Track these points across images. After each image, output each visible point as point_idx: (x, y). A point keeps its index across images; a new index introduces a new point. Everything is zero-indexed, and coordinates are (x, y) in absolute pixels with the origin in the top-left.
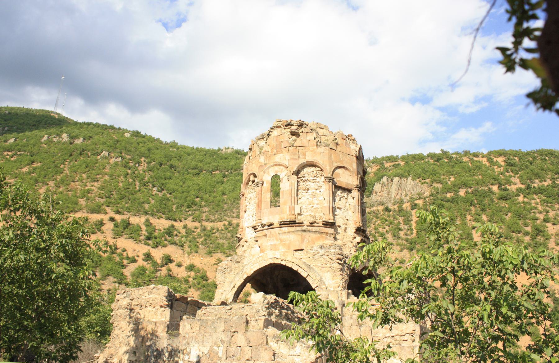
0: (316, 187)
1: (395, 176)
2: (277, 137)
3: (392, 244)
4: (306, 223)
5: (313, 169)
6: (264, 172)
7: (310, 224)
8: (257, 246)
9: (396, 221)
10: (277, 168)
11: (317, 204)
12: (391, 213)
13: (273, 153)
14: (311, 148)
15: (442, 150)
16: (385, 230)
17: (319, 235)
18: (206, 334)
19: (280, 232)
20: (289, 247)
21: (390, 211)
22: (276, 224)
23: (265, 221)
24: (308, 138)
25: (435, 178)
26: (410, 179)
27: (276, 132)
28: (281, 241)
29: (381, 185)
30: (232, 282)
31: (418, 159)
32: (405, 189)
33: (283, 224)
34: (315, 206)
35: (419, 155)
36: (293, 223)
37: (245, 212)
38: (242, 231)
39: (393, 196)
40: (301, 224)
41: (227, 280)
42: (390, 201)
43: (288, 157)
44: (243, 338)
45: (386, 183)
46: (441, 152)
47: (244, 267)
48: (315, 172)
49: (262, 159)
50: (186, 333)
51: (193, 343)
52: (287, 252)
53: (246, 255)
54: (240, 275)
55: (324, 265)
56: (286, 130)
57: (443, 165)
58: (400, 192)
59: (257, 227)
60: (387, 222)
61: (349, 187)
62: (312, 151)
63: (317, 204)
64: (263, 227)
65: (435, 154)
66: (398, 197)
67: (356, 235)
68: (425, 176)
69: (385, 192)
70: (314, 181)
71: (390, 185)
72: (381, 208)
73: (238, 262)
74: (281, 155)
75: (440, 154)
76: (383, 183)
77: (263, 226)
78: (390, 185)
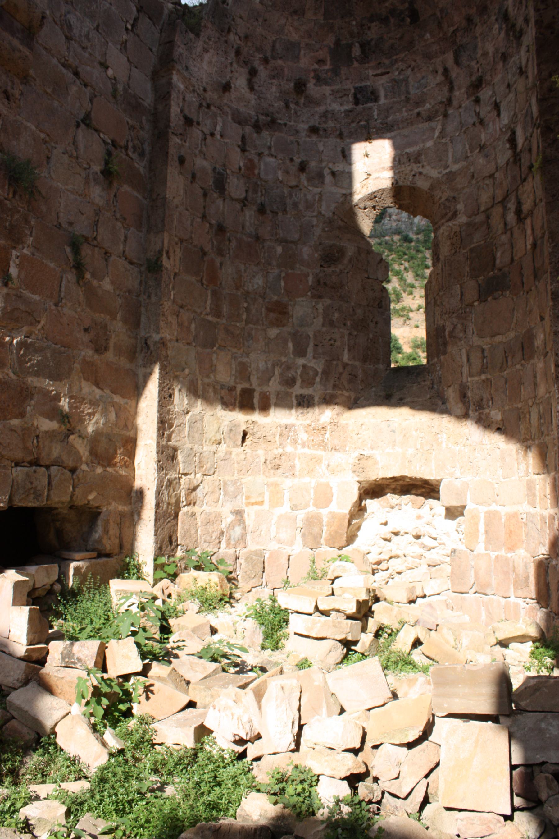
3: (413, 286)
9: (420, 255)
12: (413, 244)
16: (402, 268)
21: (410, 241)
42: (412, 228)
60: (406, 257)
72: (396, 238)
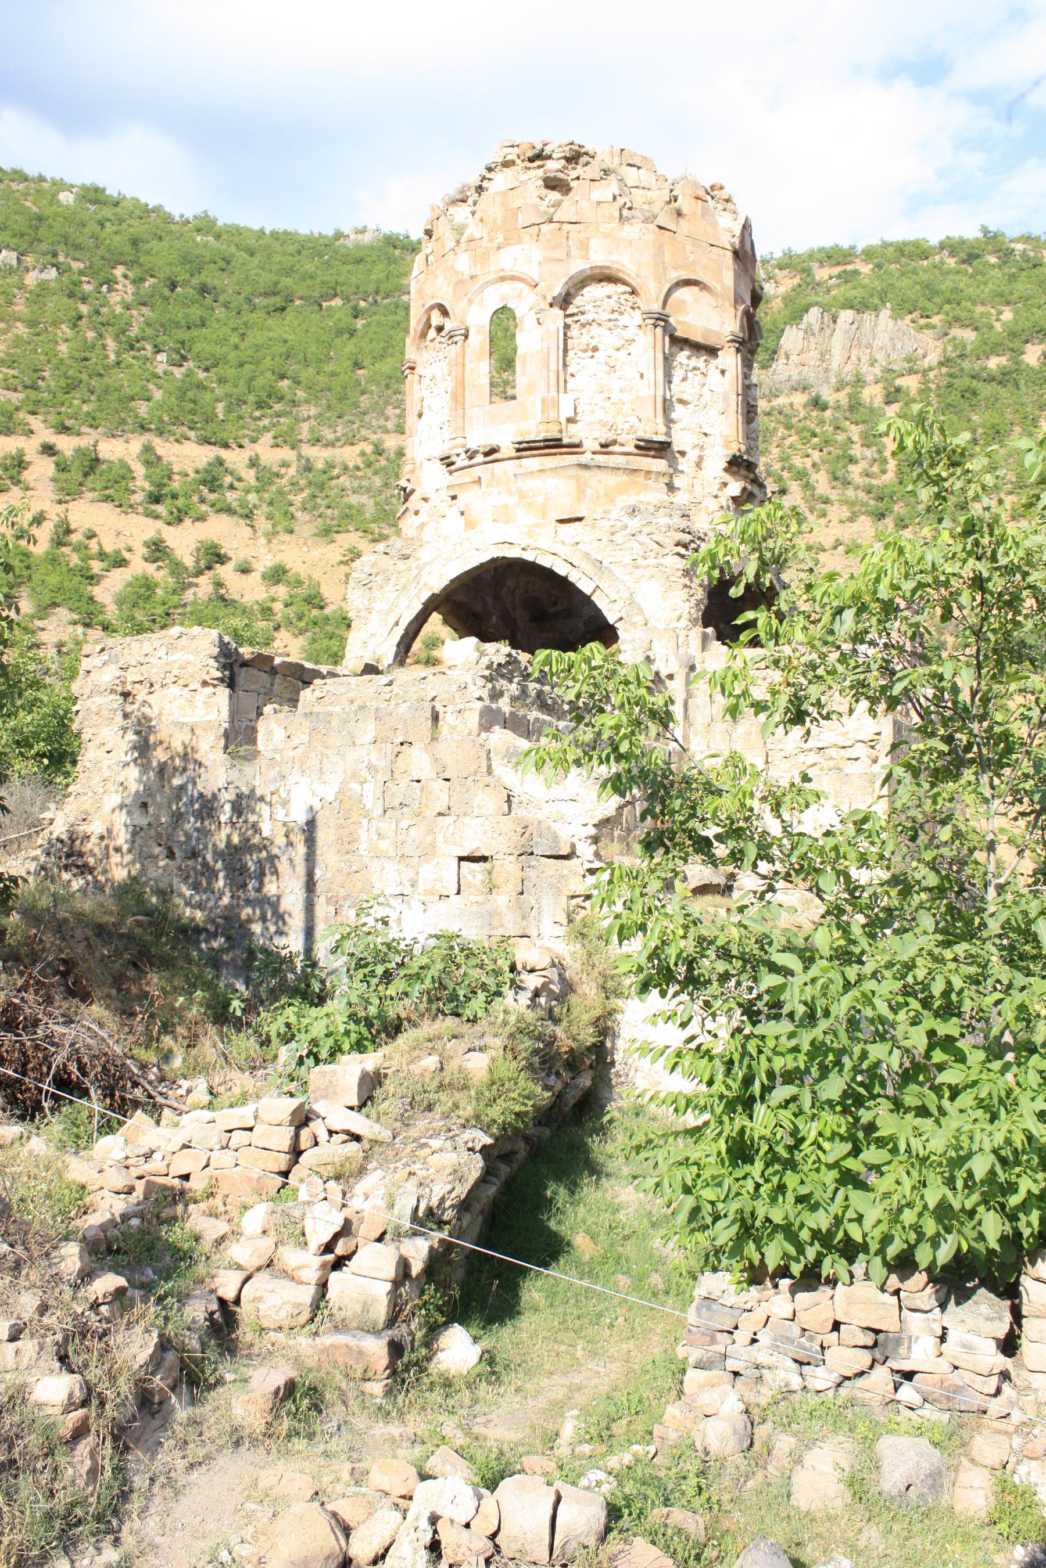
0: (618, 344)
1: (844, 307)
2: (504, 194)
3: (826, 501)
4: (590, 445)
5: (609, 288)
6: (470, 301)
7: (602, 446)
8: (454, 512)
9: (841, 437)
10: (506, 287)
11: (621, 391)
12: (828, 413)
13: (495, 244)
14: (603, 228)
15: (985, 231)
16: (808, 462)
17: (625, 478)
18: (329, 752)
19: (520, 471)
20: (544, 514)
21: (824, 408)
22: (507, 450)
23: (478, 441)
24: (596, 196)
25: (958, 312)
26: (885, 314)
27: (501, 180)
28: (522, 495)
29: (801, 333)
30: (390, 611)
31: (910, 257)
32: (869, 346)
33: (526, 448)
34: (614, 399)
35: (916, 244)
36: (553, 445)
37: (420, 415)
38: (412, 471)
39: (834, 366)
40: (575, 447)
41: (377, 606)
42: (827, 380)
43: (537, 253)
44: (425, 758)
45: (816, 328)
46: (980, 235)
47: (420, 569)
48: (615, 298)
49: (463, 263)
50: (275, 751)
51: (296, 775)
52: (538, 526)
53: (425, 537)
54: (413, 591)
55: (641, 562)
56: (532, 173)
57: (983, 274)
58: (855, 352)
59: (454, 459)
60: (816, 440)
61: (711, 342)
62: (606, 236)
63: (621, 391)
64: (471, 458)
65: (962, 242)
66: (849, 368)
67: (727, 478)
68: (929, 305)
69: (814, 354)
70: (613, 324)
71: (828, 332)
73: (406, 557)
74: (518, 248)
75: (977, 240)
76: (810, 325)
77: (471, 455)
78: (828, 332)
